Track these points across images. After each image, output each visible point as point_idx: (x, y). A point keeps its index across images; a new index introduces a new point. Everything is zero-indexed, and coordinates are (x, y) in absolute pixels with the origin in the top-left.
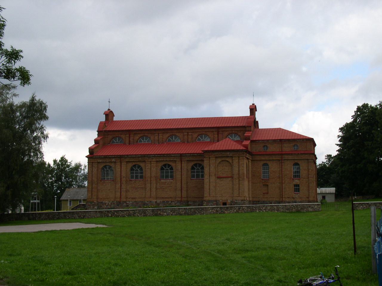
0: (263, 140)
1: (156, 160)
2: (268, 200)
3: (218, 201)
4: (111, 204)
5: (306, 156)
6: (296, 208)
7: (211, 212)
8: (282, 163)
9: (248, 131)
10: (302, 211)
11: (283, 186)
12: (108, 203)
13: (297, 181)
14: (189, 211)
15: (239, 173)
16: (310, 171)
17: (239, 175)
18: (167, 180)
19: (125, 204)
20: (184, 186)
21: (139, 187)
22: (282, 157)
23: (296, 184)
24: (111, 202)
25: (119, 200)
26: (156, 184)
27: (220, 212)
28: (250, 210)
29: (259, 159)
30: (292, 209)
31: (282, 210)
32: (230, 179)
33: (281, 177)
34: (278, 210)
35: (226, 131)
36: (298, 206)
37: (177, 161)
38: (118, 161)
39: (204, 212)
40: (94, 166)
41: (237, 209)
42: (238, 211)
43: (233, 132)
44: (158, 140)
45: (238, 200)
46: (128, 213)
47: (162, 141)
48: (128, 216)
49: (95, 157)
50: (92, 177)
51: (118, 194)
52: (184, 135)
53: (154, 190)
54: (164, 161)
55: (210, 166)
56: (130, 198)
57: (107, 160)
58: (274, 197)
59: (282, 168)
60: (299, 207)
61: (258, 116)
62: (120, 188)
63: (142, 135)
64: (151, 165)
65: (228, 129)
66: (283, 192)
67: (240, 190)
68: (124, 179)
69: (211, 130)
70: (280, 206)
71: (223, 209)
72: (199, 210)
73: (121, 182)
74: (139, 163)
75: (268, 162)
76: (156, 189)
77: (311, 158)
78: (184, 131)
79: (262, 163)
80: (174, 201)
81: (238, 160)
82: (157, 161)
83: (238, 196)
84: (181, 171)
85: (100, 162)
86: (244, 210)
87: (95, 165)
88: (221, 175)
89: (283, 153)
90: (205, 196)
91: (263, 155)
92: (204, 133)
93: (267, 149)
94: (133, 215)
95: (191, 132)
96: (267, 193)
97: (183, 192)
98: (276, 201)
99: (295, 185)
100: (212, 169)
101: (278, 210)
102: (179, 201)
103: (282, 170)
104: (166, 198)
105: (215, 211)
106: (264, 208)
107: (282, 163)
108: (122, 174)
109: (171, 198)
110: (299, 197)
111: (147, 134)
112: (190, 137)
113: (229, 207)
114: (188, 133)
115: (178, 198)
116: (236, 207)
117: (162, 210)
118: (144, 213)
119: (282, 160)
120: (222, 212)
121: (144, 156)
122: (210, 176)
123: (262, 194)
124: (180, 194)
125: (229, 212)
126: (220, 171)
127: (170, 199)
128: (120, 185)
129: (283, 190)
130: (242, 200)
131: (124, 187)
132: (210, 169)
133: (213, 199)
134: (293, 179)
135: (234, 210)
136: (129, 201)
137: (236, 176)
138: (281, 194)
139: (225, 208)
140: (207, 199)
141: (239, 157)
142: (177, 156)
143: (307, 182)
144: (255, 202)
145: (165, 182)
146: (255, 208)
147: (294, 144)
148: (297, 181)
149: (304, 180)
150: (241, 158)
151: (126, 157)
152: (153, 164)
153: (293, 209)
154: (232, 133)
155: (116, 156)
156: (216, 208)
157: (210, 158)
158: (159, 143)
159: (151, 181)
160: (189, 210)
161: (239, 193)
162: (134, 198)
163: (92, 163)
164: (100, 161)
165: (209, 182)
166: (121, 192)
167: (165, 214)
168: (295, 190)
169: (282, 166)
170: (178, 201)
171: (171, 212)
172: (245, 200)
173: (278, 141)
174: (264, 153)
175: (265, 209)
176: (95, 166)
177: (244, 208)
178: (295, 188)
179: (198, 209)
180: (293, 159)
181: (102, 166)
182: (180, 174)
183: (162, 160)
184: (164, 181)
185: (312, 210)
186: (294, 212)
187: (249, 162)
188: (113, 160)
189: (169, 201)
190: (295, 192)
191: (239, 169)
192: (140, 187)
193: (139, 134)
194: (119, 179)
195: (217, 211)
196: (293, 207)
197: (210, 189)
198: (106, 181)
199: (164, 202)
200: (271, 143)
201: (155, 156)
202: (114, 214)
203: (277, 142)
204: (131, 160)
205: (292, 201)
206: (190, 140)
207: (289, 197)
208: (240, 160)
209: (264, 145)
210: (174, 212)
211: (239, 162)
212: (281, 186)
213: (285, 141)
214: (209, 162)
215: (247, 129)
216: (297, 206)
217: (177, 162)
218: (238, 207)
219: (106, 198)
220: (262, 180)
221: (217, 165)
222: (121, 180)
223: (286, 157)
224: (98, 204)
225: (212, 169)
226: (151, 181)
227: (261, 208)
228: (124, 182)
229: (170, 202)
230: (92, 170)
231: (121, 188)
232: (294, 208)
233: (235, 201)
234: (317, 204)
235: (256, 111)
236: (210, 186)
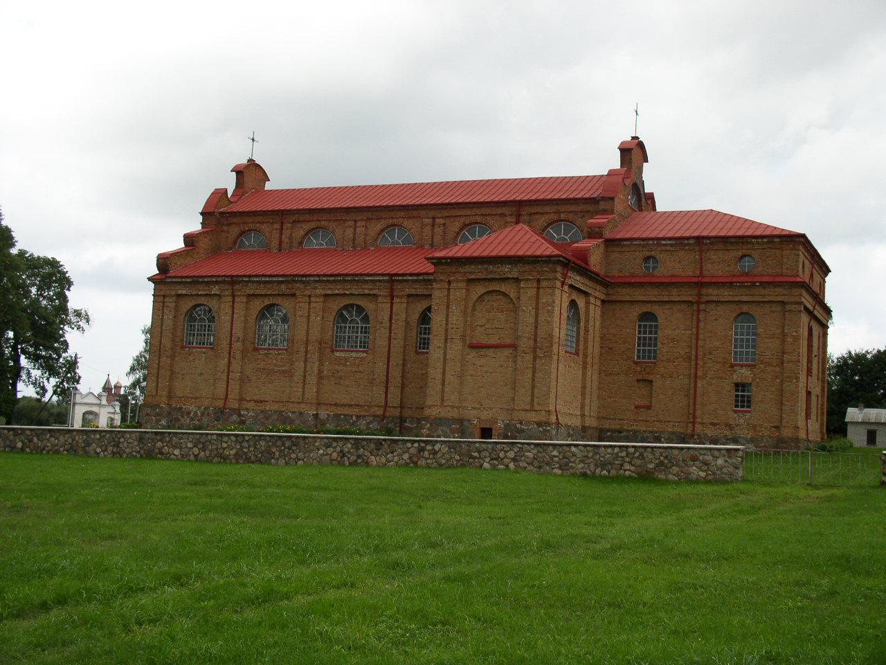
0: (643, 239)
1: (323, 292)
2: (651, 429)
3: (466, 423)
4: (203, 414)
5: (779, 290)
6: (638, 462)
7: (323, 455)
8: (698, 314)
9: (605, 212)
10: (662, 476)
11: (699, 385)
12: (196, 412)
13: (744, 374)
14: (252, 449)
15: (536, 335)
16: (789, 339)
17: (535, 340)
18: (352, 351)
19: (235, 417)
20: (396, 373)
21: (276, 369)
22: (699, 295)
23: (739, 381)
25: (220, 403)
26: (321, 363)
27: (353, 458)
28: (457, 457)
29: (628, 298)
30: (622, 465)
31: (581, 465)
32: (507, 352)
33: (693, 357)
34: (567, 464)
35: (542, 214)
36: (648, 455)
37: (380, 295)
38: (227, 293)
39: (301, 455)
40: (168, 307)
41: (413, 451)
42: (415, 459)
43: (562, 216)
44: (354, 240)
45: (528, 423)
46: (70, 441)
47: (365, 242)
48: (67, 451)
49: (170, 280)
50: (161, 337)
51: (221, 386)
52: (422, 227)
53: (312, 379)
54: (345, 294)
55: (448, 307)
57: (199, 290)
58: (669, 422)
59: (698, 327)
60: (650, 456)
61: (652, 178)
63: (312, 225)
64: (310, 305)
65: (547, 209)
66: (697, 406)
67: (536, 390)
68: (237, 346)
69: (500, 211)
70: (573, 449)
71: (363, 447)
72: (283, 444)
73: (230, 353)
75: (655, 309)
76: (320, 377)
77: (793, 299)
78: (423, 213)
79: (637, 310)
80: (364, 416)
81: (534, 291)
82: (326, 295)
83: (528, 407)
84: (391, 326)
85: (181, 295)
86: (439, 455)
87: (171, 303)
88: (485, 340)
89: (705, 280)
90: (429, 403)
91: (642, 285)
92: (479, 219)
93: (654, 268)
94: (84, 448)
95: (445, 218)
96: (649, 407)
97: (391, 389)
98: (673, 433)
99: (737, 385)
100: (456, 318)
101: (567, 464)
102: (378, 416)
103: (697, 334)
104: (344, 405)
105: (335, 455)
106: (511, 454)
107: (699, 311)
109: (357, 406)
110: (748, 424)
111: (326, 224)
112: (438, 230)
113: (385, 440)
114: (434, 218)
115: (376, 409)
116: (409, 445)
117: (167, 439)
118: (114, 446)
119: (698, 303)
120: (359, 461)
121: (292, 279)
122: (446, 340)
123: (633, 408)
124: (383, 397)
125: (383, 460)
126: (481, 326)
127: (355, 411)
129: (699, 399)
130: (539, 424)
131: (236, 366)
132: (447, 315)
133: (449, 415)
134: (732, 366)
135: (400, 455)
136: (247, 409)
137: (525, 344)
138: (691, 411)
139: (372, 446)
140: (433, 412)
141: (539, 281)
142: (380, 281)
143: (777, 377)
144: (609, 434)
145: (346, 359)
146: (479, 452)
147: (740, 253)
148: (744, 370)
149: (769, 369)
150: (544, 284)
151: (248, 282)
152: (317, 302)
153: (627, 466)
154: (557, 221)
155: (220, 279)
156: (341, 443)
157: (449, 282)
158: (354, 247)
159: (306, 352)
160: (252, 443)
161: (532, 400)
162: (261, 402)
163: (164, 296)
164: (184, 292)
165: (442, 360)
166: (228, 382)
167: (177, 452)
168: (737, 401)
169: (698, 321)
170: (375, 416)
171: (195, 446)
172: (548, 424)
173: (691, 241)
174: (647, 280)
175: (514, 460)
176: (169, 304)
177: (437, 447)
178: (737, 396)
179: (279, 443)
180: (737, 299)
181: (186, 305)
182: (388, 335)
183: (341, 292)
184: (342, 354)
185: (703, 474)
186: (630, 477)
187: (588, 303)
188: (215, 290)
189: (352, 416)
190: (736, 406)
191: (536, 322)
193: (305, 221)
194: (225, 344)
195: (343, 454)
196: (627, 455)
197: (444, 380)
198: (194, 350)
199: (337, 416)
200: (669, 248)
201: (322, 279)
202: (31, 441)
203: (689, 244)
204: (258, 292)
205: (725, 436)
206: (437, 239)
207: (715, 421)
208: (541, 290)
209: (648, 254)
210: (204, 449)
211: (537, 298)
212: (692, 385)
213: (711, 244)
214: (448, 296)
215: (602, 205)
216: (642, 455)
217: (380, 299)
218: (416, 445)
220: (636, 363)
221: (470, 305)
222: (230, 348)
223: (713, 294)
224: (169, 413)
225: (455, 318)
226: (306, 355)
227: (502, 455)
228: (238, 355)
229: (354, 418)
230: (163, 316)
231: (228, 372)
232: (630, 463)
233: (518, 425)
234: (728, 450)
235: (646, 160)
236: (444, 374)
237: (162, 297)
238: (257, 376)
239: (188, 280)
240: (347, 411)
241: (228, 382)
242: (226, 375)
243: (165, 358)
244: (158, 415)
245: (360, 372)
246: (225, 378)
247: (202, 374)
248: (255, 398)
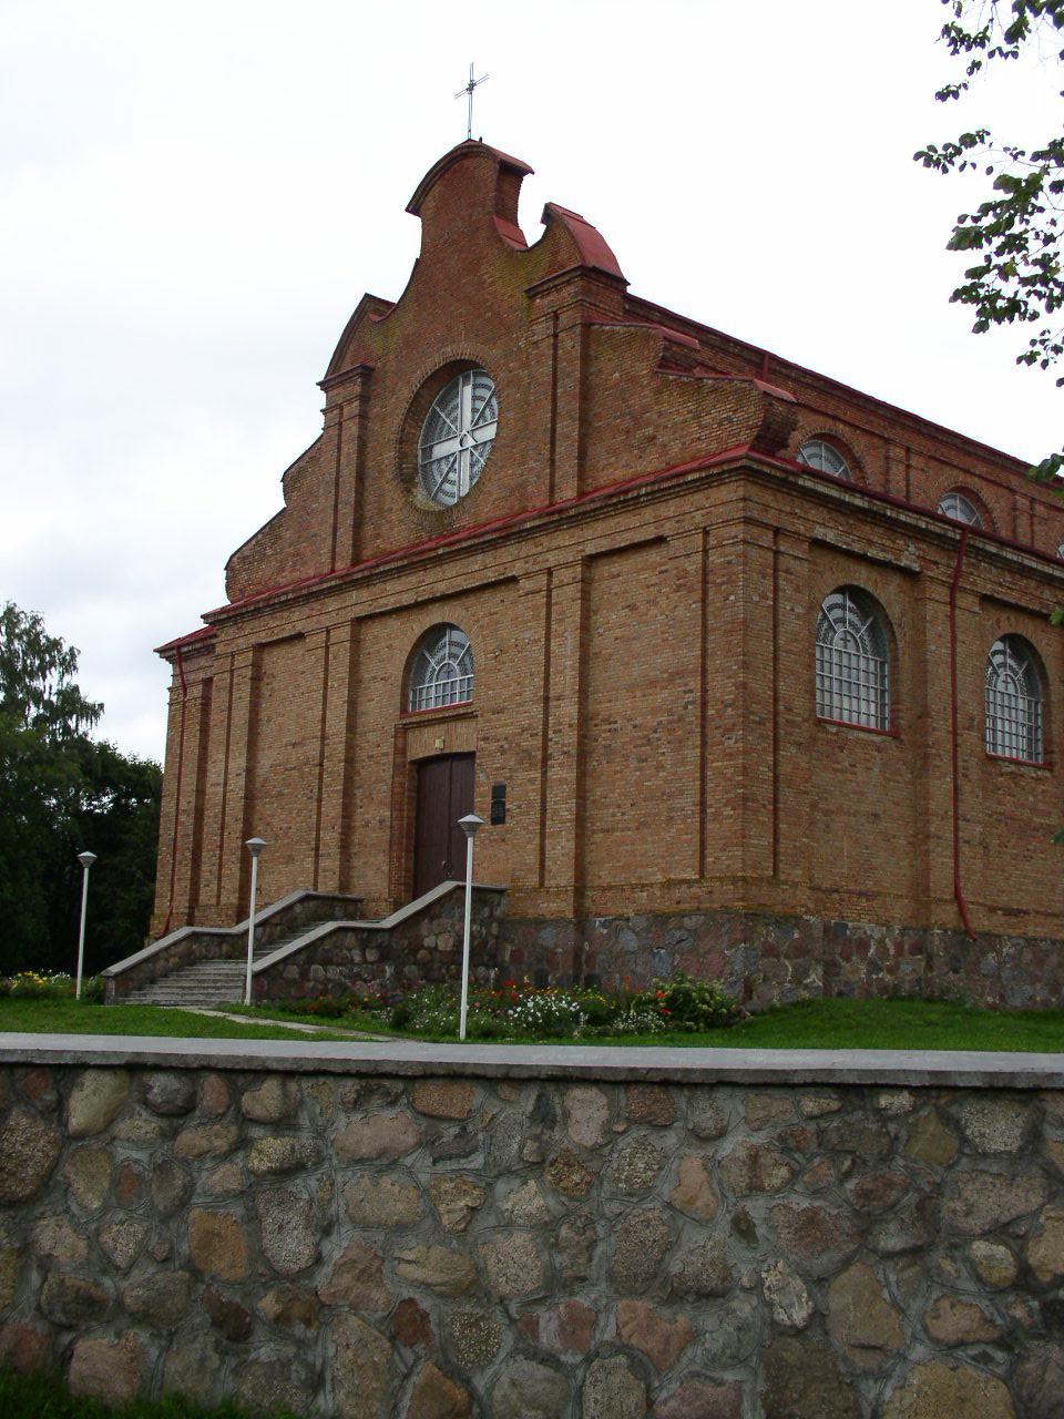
57: (871, 543)
62: (951, 813)
73: (955, 758)
163: (777, 532)
164: (831, 537)
188: (909, 556)
222: (956, 746)
237: (771, 534)
239: (858, 502)
241: (956, 848)
246: (949, 835)
247: (876, 816)
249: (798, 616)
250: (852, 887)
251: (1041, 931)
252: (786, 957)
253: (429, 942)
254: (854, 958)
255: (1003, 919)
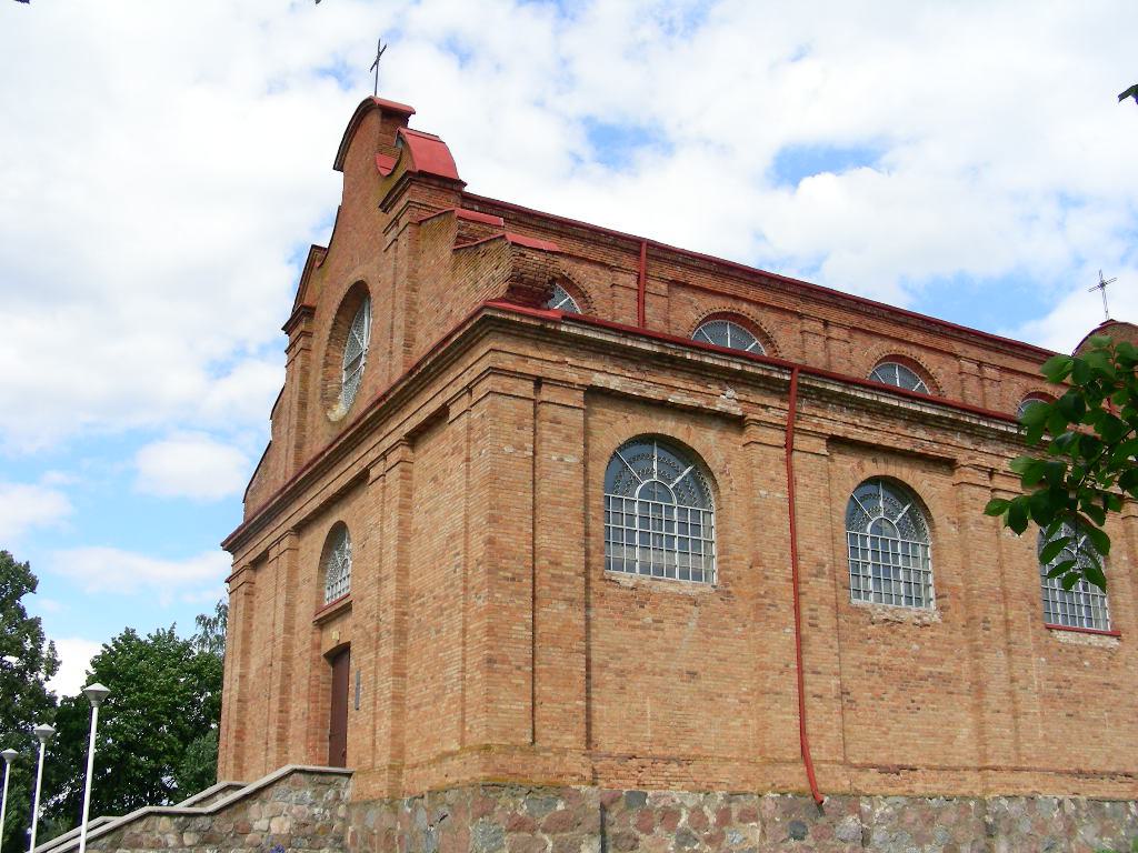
4: (724, 817)
12: (697, 812)
21: (924, 669)
24: (720, 795)
25: (795, 777)
40: (555, 421)
56: (864, 768)
62: (794, 666)
73: (797, 608)
74: (902, 472)
108: (801, 544)
128: (790, 630)
145: (1080, 651)
162: (898, 770)
163: (539, 382)
164: (615, 384)
188: (727, 400)
192: (931, 675)
199: (1097, 803)
219: (668, 761)
222: (797, 594)
228: (826, 620)
237: (530, 385)
238: (871, 688)
240: (1106, 789)
242: (795, 680)
243: (562, 607)
244: (561, 824)
245: (1115, 687)
246: (793, 690)
247: (693, 674)
248: (880, 757)
249: (568, 466)
250: (658, 751)
251: (933, 788)
252: (545, 831)
253: (260, 825)
254: (657, 829)
255: (878, 777)
